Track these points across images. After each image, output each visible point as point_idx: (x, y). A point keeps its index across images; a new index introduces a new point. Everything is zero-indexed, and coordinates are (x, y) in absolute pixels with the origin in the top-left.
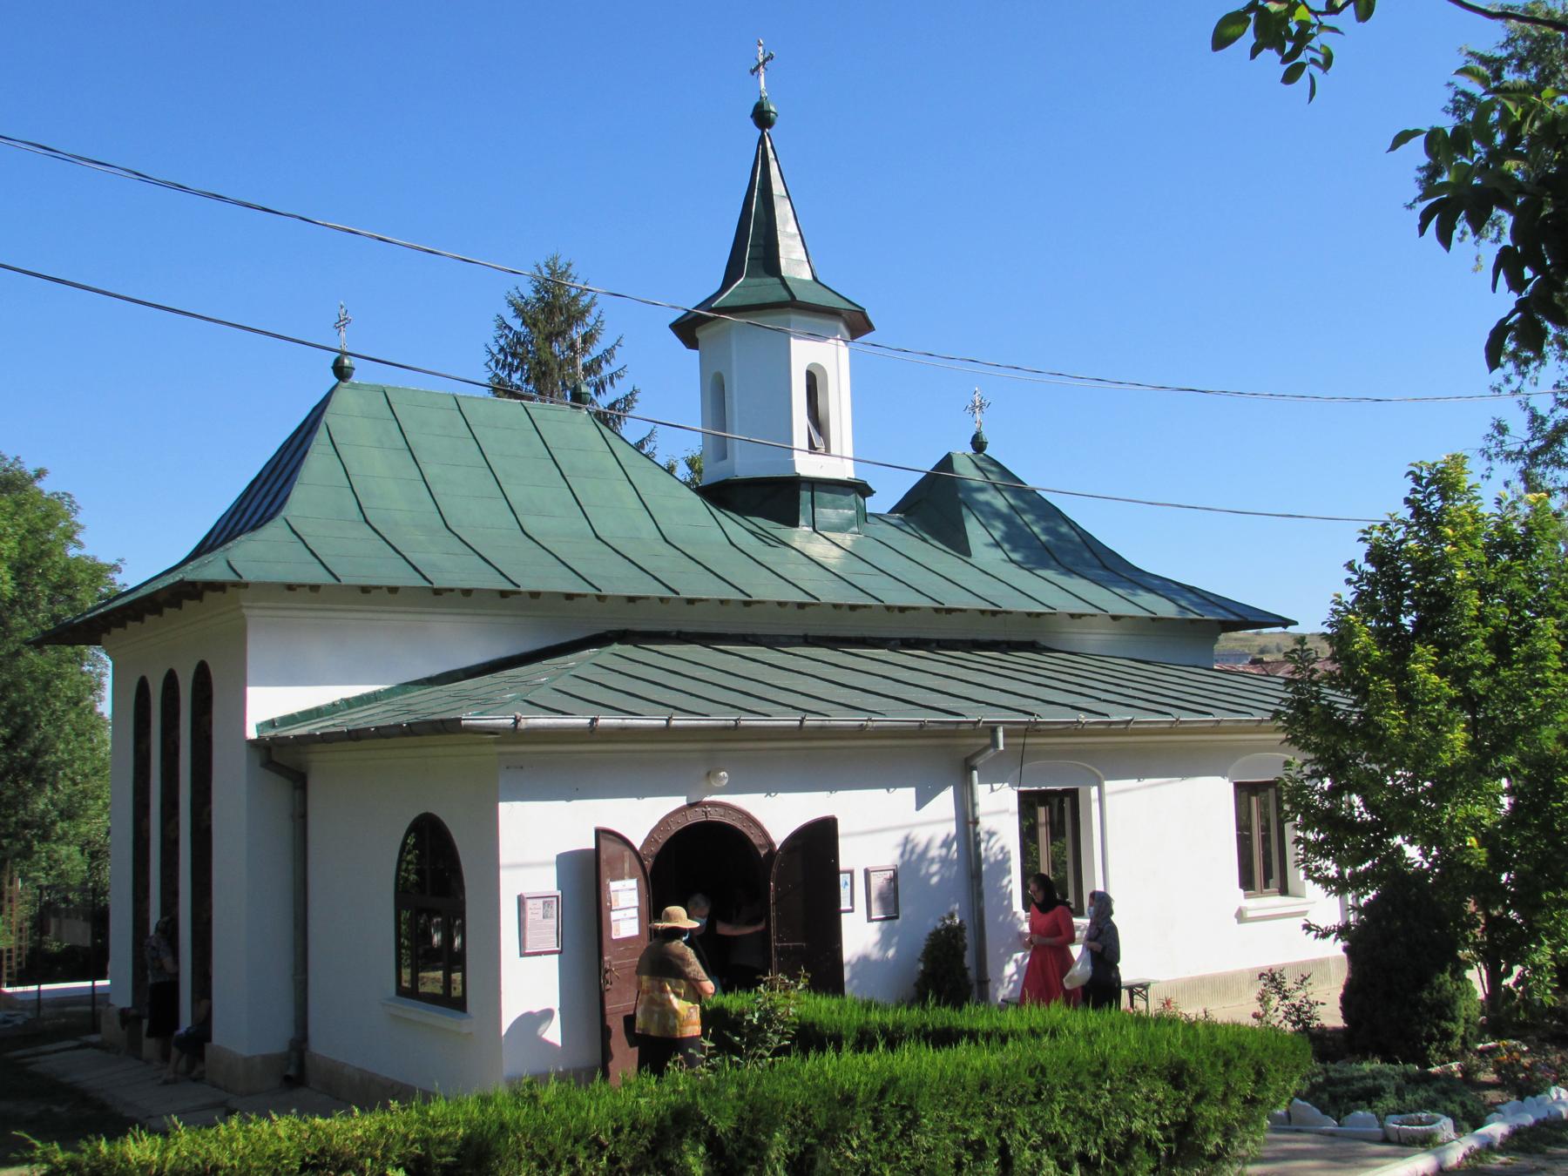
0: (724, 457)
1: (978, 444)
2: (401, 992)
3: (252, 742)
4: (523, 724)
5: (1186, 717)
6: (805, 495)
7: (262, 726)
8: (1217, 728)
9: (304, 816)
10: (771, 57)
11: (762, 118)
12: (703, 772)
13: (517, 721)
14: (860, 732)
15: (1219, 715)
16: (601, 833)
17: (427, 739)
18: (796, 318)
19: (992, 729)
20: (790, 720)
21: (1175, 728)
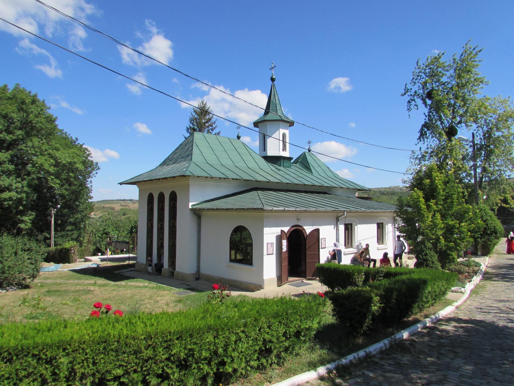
0: (265, 151)
1: (309, 151)
2: (231, 260)
3: (190, 209)
4: (273, 209)
5: (374, 210)
6: (282, 160)
7: (192, 206)
8: (378, 212)
9: (200, 224)
10: (275, 66)
11: (273, 80)
12: (296, 219)
13: (272, 209)
14: (325, 212)
15: (378, 210)
16: (282, 231)
17: (242, 211)
18: (281, 123)
19: (344, 211)
20: (314, 209)
21: (371, 212)
